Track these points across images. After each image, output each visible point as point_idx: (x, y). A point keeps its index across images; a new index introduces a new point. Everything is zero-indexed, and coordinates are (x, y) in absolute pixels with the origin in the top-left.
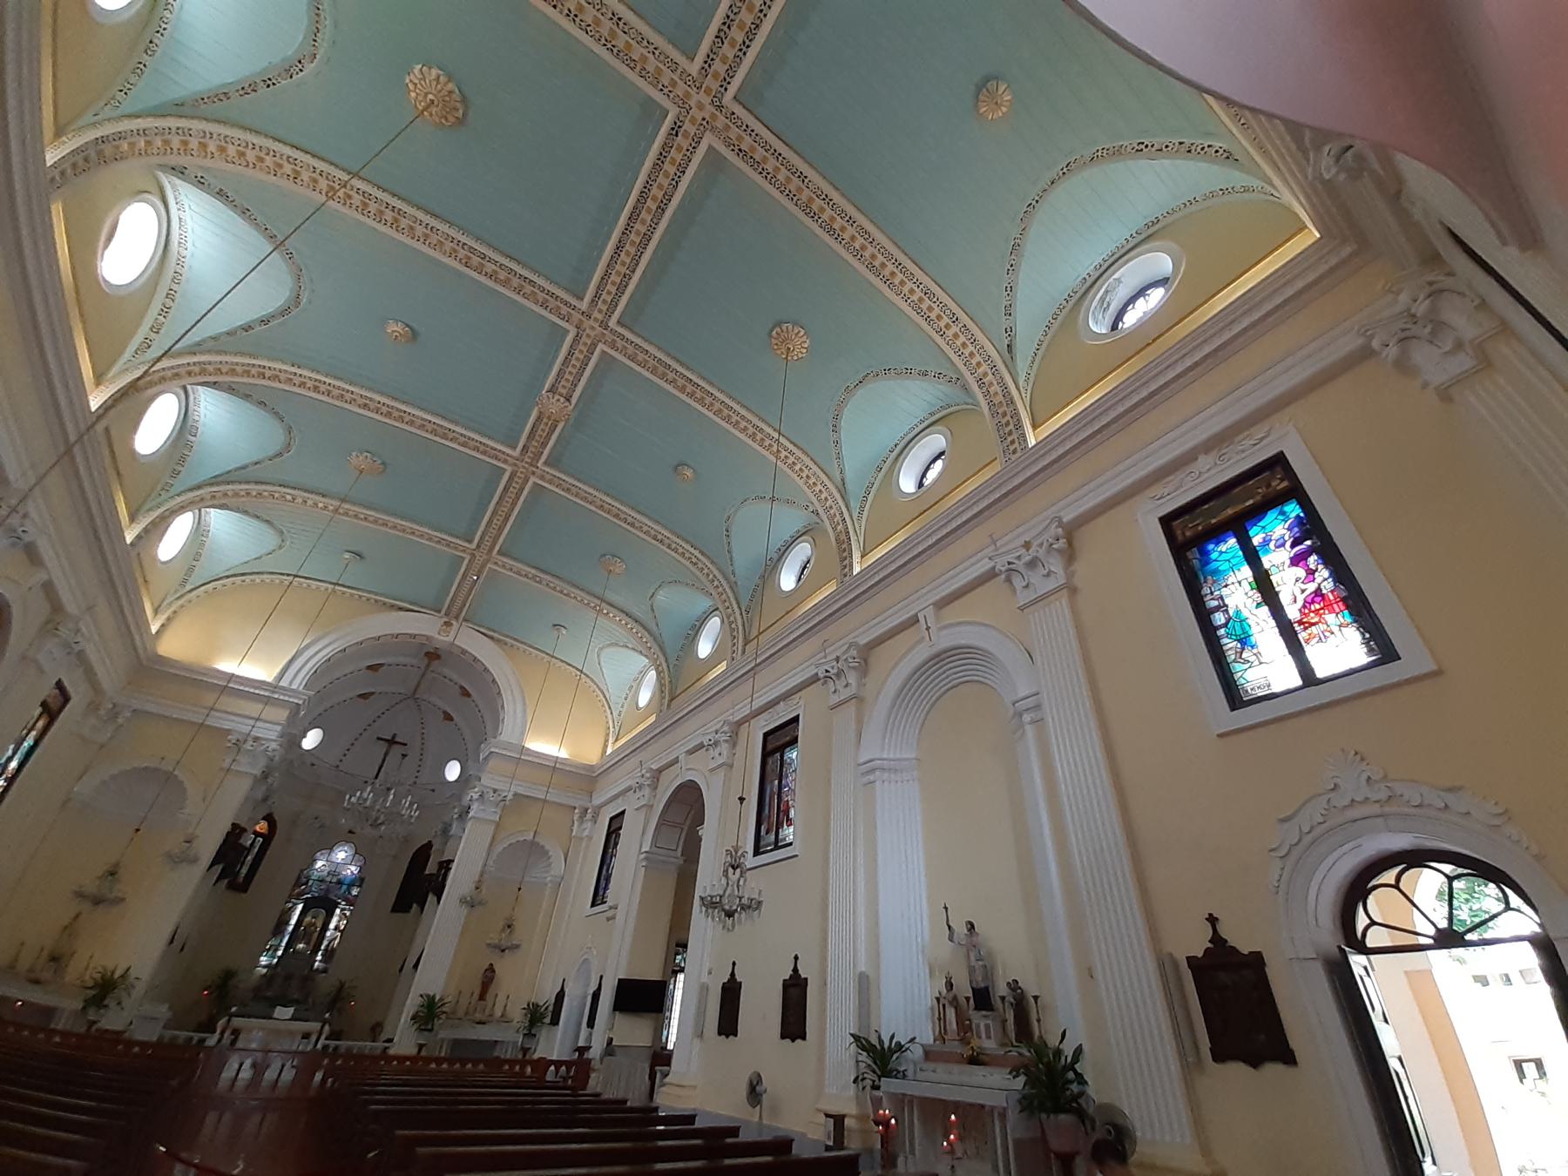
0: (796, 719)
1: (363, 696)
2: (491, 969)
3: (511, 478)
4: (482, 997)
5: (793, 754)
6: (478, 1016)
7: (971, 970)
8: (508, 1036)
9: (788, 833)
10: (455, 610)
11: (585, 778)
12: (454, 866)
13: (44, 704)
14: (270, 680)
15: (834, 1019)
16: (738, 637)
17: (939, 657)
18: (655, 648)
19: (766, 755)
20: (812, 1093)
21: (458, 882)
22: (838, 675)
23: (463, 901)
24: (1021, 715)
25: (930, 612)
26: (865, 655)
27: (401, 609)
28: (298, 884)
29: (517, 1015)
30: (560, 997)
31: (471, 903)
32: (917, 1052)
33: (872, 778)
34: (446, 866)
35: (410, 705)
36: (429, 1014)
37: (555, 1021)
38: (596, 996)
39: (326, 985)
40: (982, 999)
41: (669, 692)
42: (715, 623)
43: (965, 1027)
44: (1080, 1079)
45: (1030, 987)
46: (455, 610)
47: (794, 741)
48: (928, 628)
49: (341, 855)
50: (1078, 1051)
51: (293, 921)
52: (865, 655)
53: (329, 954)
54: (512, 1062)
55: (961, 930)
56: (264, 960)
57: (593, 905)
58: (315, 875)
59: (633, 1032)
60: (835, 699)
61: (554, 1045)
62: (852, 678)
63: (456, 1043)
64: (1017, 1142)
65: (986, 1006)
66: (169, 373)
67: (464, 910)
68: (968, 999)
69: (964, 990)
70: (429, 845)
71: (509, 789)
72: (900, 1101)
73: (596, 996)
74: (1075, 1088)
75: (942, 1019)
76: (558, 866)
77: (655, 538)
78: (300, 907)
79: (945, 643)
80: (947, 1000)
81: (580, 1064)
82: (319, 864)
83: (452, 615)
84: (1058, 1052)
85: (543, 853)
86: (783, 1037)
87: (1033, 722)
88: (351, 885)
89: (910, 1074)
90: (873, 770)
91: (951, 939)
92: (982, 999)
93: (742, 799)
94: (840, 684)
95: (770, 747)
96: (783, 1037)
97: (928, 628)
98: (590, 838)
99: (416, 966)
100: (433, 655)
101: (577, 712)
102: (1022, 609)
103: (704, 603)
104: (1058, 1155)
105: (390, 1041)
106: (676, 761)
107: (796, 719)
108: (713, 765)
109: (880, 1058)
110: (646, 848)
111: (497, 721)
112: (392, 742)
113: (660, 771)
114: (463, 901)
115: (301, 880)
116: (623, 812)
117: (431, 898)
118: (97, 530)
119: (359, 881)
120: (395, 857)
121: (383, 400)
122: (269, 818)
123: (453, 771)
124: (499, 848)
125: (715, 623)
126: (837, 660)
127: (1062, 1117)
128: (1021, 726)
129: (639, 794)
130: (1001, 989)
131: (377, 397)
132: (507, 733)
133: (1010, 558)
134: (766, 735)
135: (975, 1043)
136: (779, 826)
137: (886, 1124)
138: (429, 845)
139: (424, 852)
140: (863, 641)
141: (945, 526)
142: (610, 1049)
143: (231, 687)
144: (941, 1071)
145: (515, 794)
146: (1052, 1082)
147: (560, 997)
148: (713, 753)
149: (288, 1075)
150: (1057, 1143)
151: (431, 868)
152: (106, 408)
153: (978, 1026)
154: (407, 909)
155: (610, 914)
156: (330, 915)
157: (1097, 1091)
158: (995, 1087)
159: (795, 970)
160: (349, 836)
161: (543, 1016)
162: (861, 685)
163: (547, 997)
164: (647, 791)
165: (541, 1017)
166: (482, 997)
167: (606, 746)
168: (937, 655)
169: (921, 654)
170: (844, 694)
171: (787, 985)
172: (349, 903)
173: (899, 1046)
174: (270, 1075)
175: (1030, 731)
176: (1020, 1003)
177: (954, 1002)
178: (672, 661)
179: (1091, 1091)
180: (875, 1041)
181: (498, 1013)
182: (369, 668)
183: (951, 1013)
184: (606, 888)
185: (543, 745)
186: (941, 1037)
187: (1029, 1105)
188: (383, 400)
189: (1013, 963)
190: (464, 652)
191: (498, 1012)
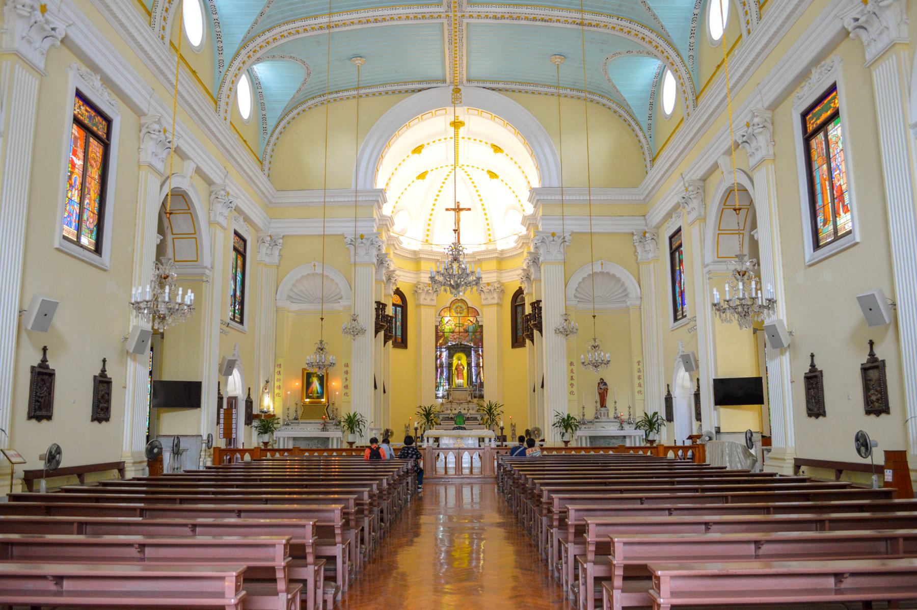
2: (602, 382)
4: (603, 404)
9: (845, 221)
12: (542, 304)
21: (551, 318)
23: (557, 331)
27: (414, 91)
28: (438, 337)
34: (536, 306)
37: (670, 418)
38: (697, 396)
57: (676, 320)
59: (740, 420)
63: (592, 438)
67: (561, 339)
70: (520, 292)
73: (697, 396)
95: (811, 128)
99: (542, 386)
105: (543, 440)
106: (715, 167)
113: (704, 179)
114: (557, 331)
116: (679, 230)
120: (499, 305)
129: (688, 209)
134: (804, 115)
136: (836, 214)
145: (572, 233)
147: (669, 400)
151: (528, 310)
154: (523, 345)
155: (690, 326)
178: (685, 54)
184: (683, 304)
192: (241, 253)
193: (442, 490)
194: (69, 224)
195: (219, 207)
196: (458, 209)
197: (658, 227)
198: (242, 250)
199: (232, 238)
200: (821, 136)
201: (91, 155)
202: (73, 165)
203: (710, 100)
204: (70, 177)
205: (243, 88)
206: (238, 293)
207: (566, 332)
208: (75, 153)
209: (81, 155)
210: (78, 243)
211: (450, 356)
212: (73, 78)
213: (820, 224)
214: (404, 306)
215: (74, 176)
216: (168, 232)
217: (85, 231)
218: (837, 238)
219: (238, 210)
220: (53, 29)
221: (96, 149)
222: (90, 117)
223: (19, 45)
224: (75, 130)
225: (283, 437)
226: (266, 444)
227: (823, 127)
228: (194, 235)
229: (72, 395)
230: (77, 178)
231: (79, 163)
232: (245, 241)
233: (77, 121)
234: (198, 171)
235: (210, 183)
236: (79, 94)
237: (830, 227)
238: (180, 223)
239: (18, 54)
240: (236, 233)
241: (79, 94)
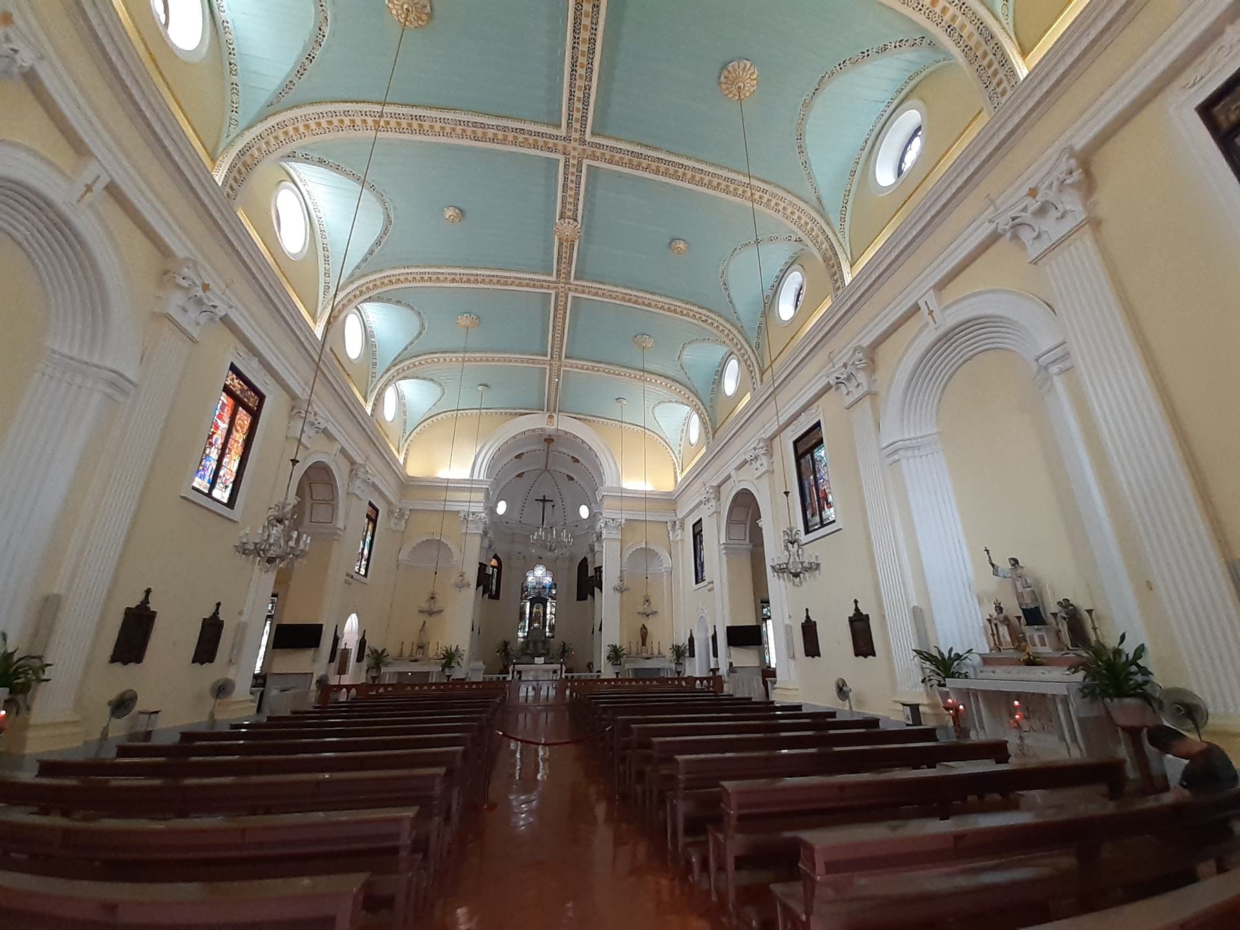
0: (818, 424)
1: (520, 476)
3: (556, 298)
4: (644, 644)
5: (821, 453)
6: (645, 655)
7: (1020, 596)
8: (666, 664)
9: (830, 513)
10: (552, 407)
11: (669, 501)
13: (368, 516)
14: (467, 477)
15: (897, 640)
16: (756, 370)
17: (947, 337)
18: (692, 397)
19: (798, 458)
20: (889, 690)
21: (610, 578)
22: (848, 379)
23: (615, 589)
24: (1046, 368)
25: (931, 298)
26: (871, 354)
27: (521, 414)
28: (523, 592)
29: (668, 654)
30: (691, 640)
31: (621, 590)
32: (977, 660)
33: (896, 457)
34: (599, 570)
35: (547, 474)
36: (616, 655)
37: (692, 655)
39: (555, 644)
40: (1034, 616)
41: (711, 427)
42: (733, 366)
43: (1018, 639)
44: (1144, 671)
45: (1081, 602)
46: (552, 407)
47: (820, 442)
48: (931, 313)
49: (540, 571)
50: (1140, 650)
51: (528, 612)
52: (871, 354)
53: (552, 628)
54: (673, 679)
55: (1005, 566)
56: (520, 634)
57: (697, 582)
58: (530, 586)
59: (745, 657)
60: (851, 399)
61: (695, 668)
62: (862, 377)
63: (636, 670)
64: (1079, 720)
65: (1029, 620)
66: (345, 301)
68: (1019, 618)
69: (1013, 609)
70: (585, 559)
71: (622, 517)
72: (966, 694)
74: (1139, 678)
75: (995, 634)
76: (667, 562)
77: (669, 310)
78: (528, 604)
79: (950, 319)
80: (999, 618)
81: (714, 678)
82: (530, 579)
83: (552, 408)
84: (1118, 652)
85: (655, 554)
86: (857, 655)
87: (1061, 372)
88: (550, 588)
89: (971, 673)
90: (896, 451)
91: (996, 573)
92: (1034, 616)
93: (787, 493)
94: (852, 386)
95: (800, 451)
96: (857, 655)
97: (931, 313)
98: (682, 540)
100: (549, 440)
101: (651, 455)
102: (1035, 262)
103: (722, 351)
104: (1124, 729)
106: (729, 477)
107: (818, 424)
108: (758, 474)
109: (943, 666)
110: (723, 541)
111: (601, 475)
112: (544, 500)
113: (719, 486)
114: (615, 589)
115: (524, 589)
117: (596, 590)
118: (351, 410)
119: (554, 586)
121: (462, 271)
122: (495, 557)
123: (584, 512)
124: (627, 555)
125: (733, 365)
126: (845, 366)
127: (1127, 700)
128: (1048, 378)
129: (708, 505)
130: (1052, 606)
131: (458, 271)
132: (609, 482)
133: (1012, 214)
134: (795, 443)
135: (1030, 649)
136: (821, 509)
137: (957, 710)
138: (585, 559)
139: (583, 564)
140: (866, 343)
141: (932, 206)
142: (732, 669)
143: (448, 486)
144: (1000, 672)
146: (1113, 674)
147: (691, 640)
148: (756, 464)
149: (552, 693)
150: (1122, 719)
151: (591, 573)
152: (325, 335)
153: (1032, 638)
156: (545, 607)
157: (1163, 677)
158: (1056, 680)
159: (857, 609)
160: (540, 560)
161: (683, 653)
162: (872, 381)
163: (683, 641)
164: (713, 502)
165: (683, 652)
166: (644, 644)
167: (676, 477)
168: (946, 334)
169: (929, 337)
170: (861, 391)
171: (851, 620)
172: (553, 598)
173: (958, 657)
174: (543, 693)
175: (1059, 384)
176: (1072, 616)
177: (1006, 621)
179: (1157, 678)
180: (936, 654)
181: (656, 653)
182: (517, 457)
183: (1003, 630)
185: (634, 483)
186: (998, 647)
187: (1087, 692)
188: (462, 271)
189: (1060, 583)
190: (566, 433)
191: (656, 653)
192: (373, 520)
193: (521, 716)
194: (202, 477)
195: (358, 483)
196: (544, 500)
197: (683, 519)
198: (373, 517)
199: (366, 509)
200: (808, 456)
201: (238, 421)
202: (217, 427)
203: (724, 433)
204: (210, 437)
205: (390, 396)
206: (366, 552)
207: (621, 590)
208: (220, 417)
209: (227, 420)
210: (209, 495)
211: (531, 607)
212: (232, 353)
213: (809, 516)
214: (499, 567)
215: (215, 436)
216: (308, 498)
217: (219, 485)
218: (823, 526)
219: (374, 485)
220: (215, 307)
221: (244, 419)
222: (242, 390)
223: (173, 311)
224: (224, 398)
225: (389, 673)
226: (374, 678)
227: (810, 451)
228: (332, 502)
229: (173, 637)
230: (219, 438)
231: (223, 426)
232: (377, 511)
233: (227, 389)
234: (343, 451)
235: (353, 463)
236: (233, 368)
237: (817, 519)
238: (320, 492)
239: (169, 317)
240: (370, 504)
241: (233, 368)
